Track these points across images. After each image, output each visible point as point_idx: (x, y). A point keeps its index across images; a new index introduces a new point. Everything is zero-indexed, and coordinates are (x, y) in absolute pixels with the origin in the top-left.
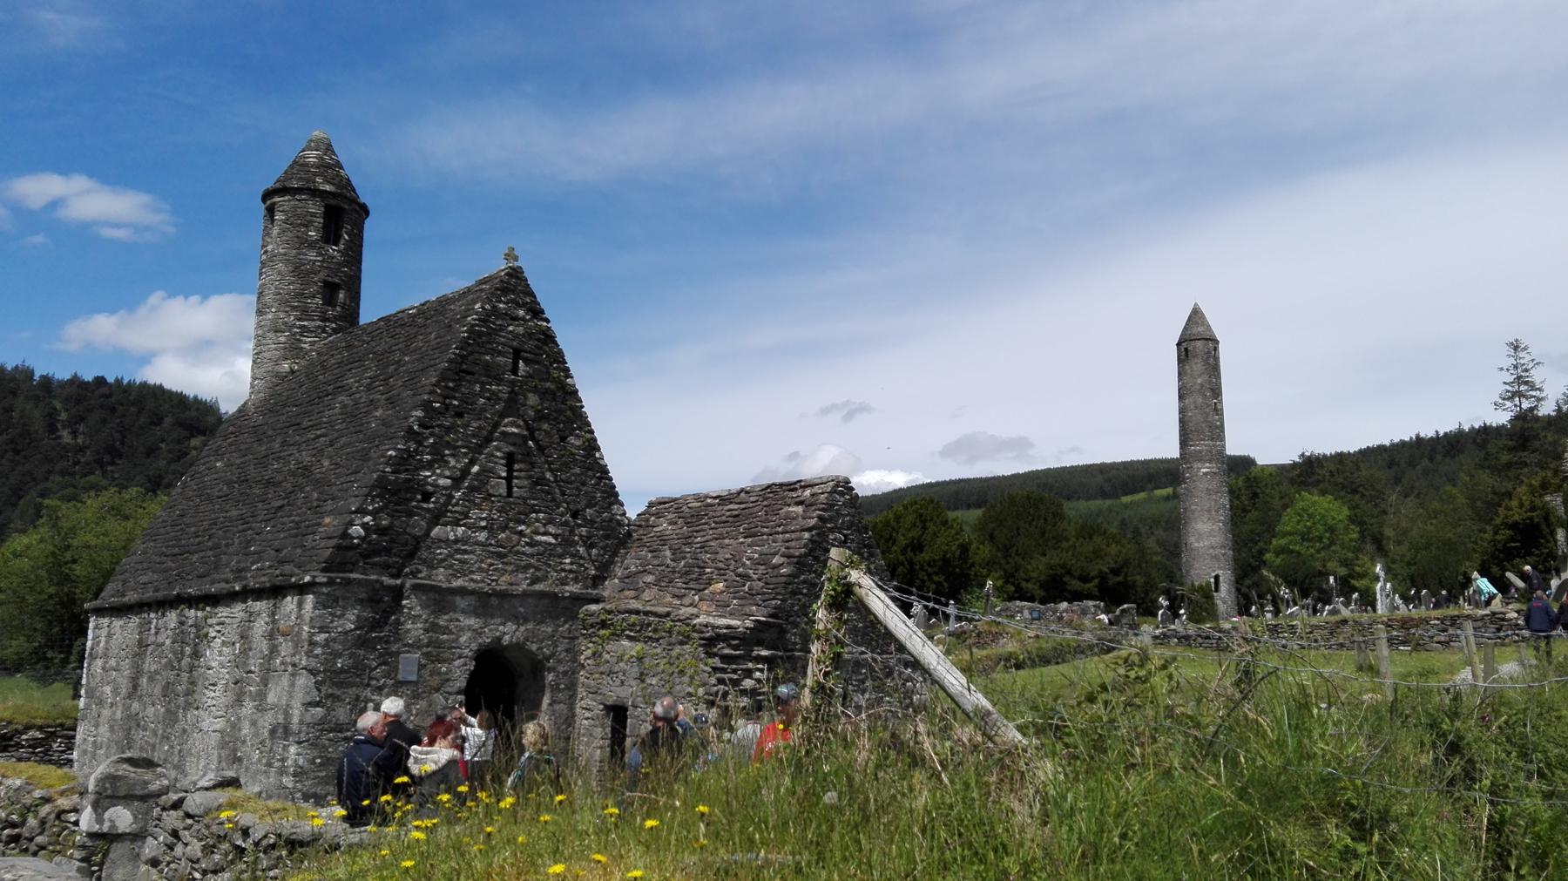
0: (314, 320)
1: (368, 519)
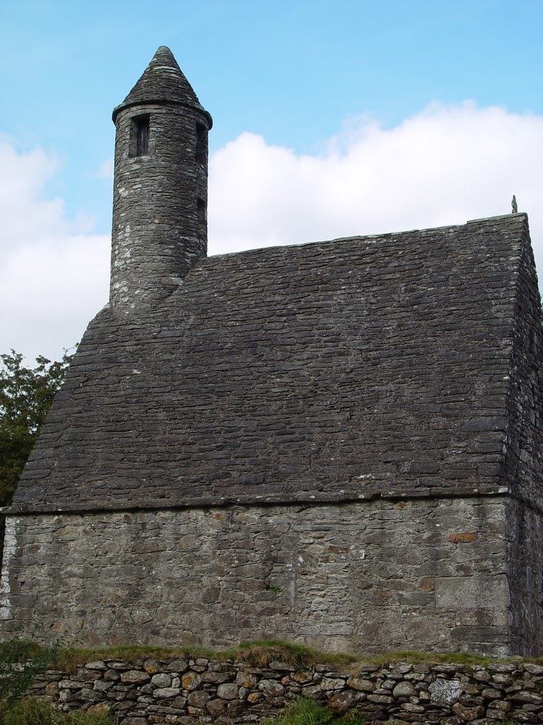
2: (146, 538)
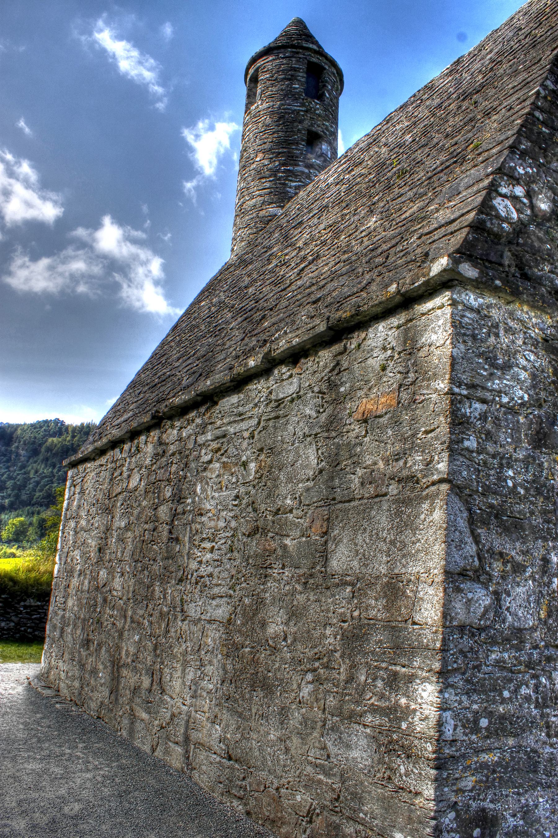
0: (298, 165)
1: (519, 191)
2: (116, 477)
